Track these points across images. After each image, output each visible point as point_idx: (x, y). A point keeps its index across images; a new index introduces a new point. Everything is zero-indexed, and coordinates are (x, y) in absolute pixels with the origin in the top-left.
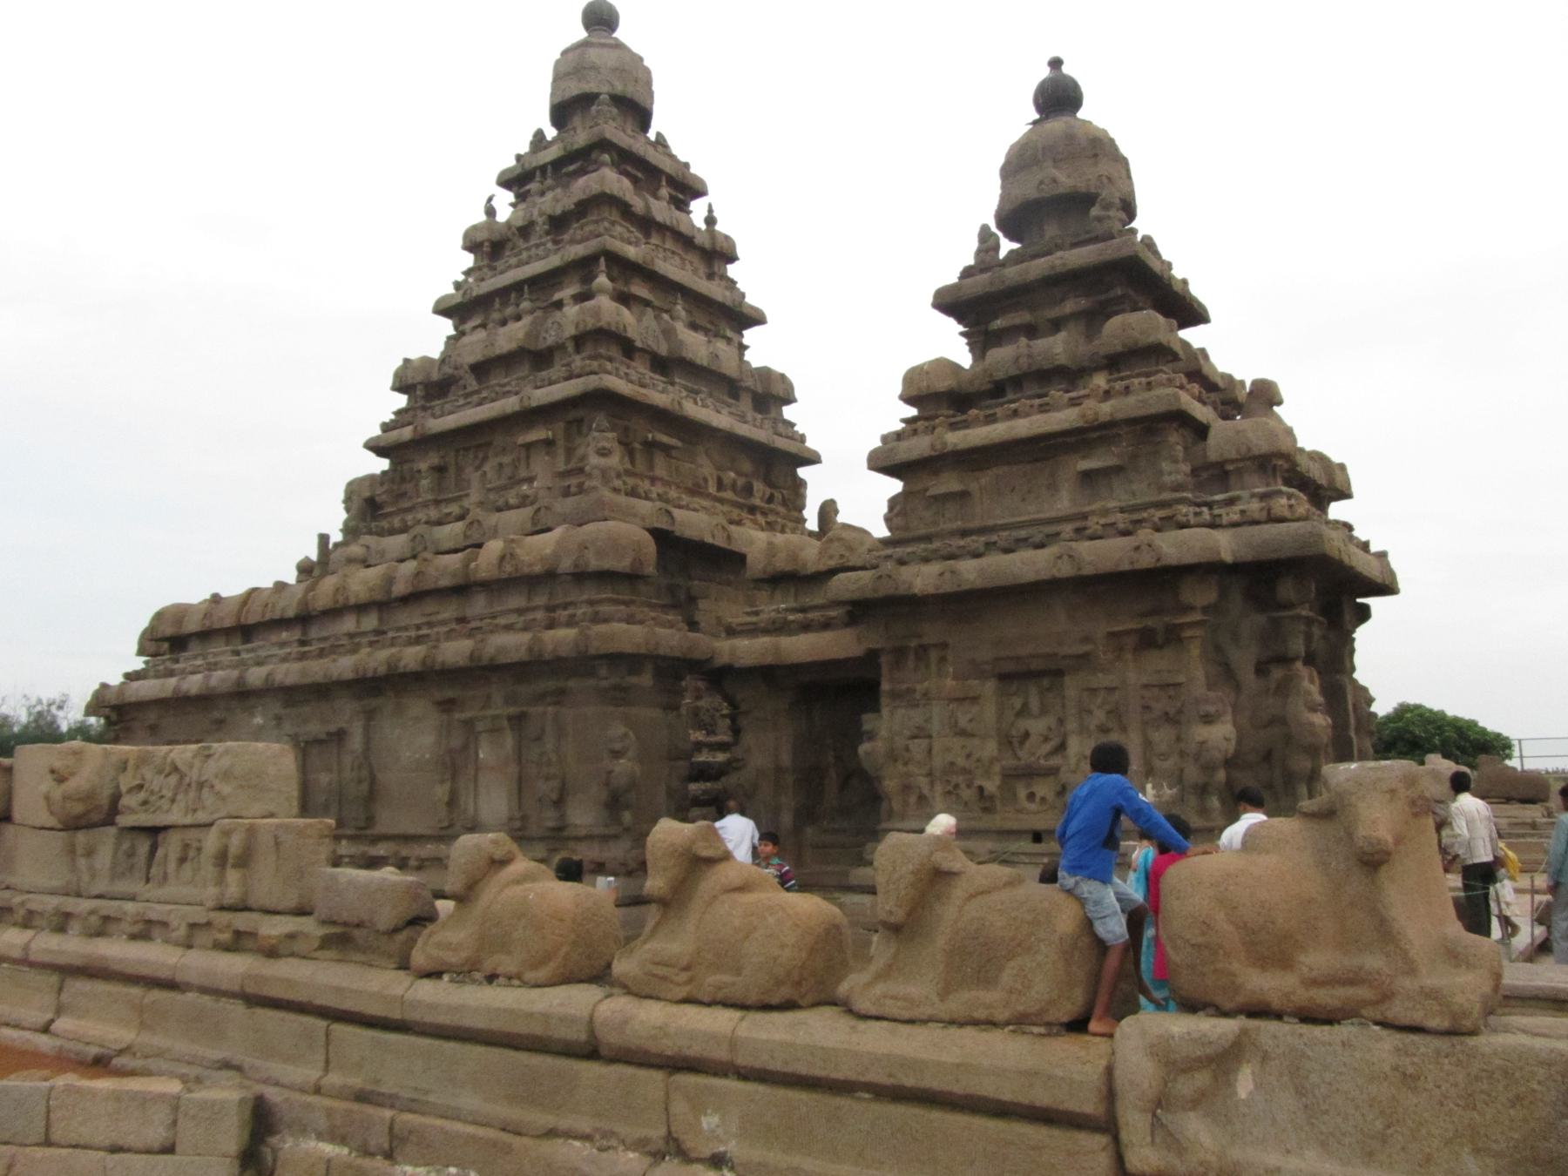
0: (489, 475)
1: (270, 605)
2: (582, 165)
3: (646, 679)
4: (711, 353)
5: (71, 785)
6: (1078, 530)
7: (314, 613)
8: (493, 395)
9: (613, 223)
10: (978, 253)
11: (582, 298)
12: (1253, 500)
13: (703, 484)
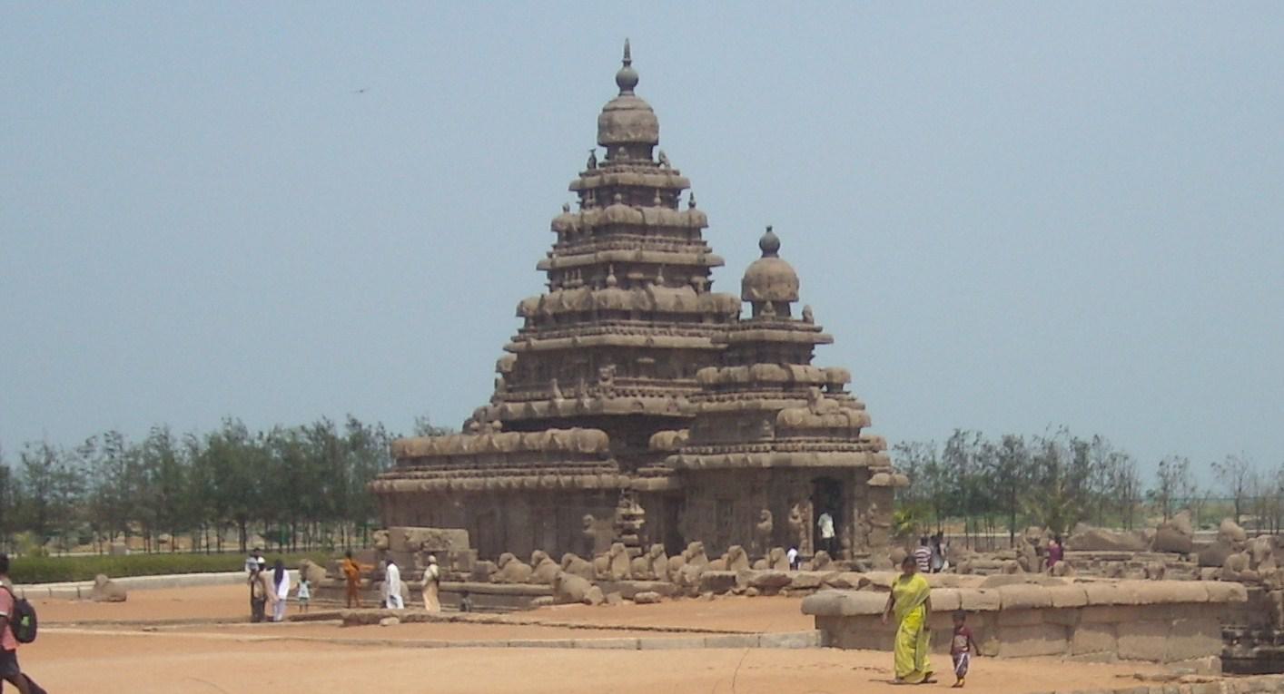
3: (602, 496)
5: (412, 540)
11: (605, 285)
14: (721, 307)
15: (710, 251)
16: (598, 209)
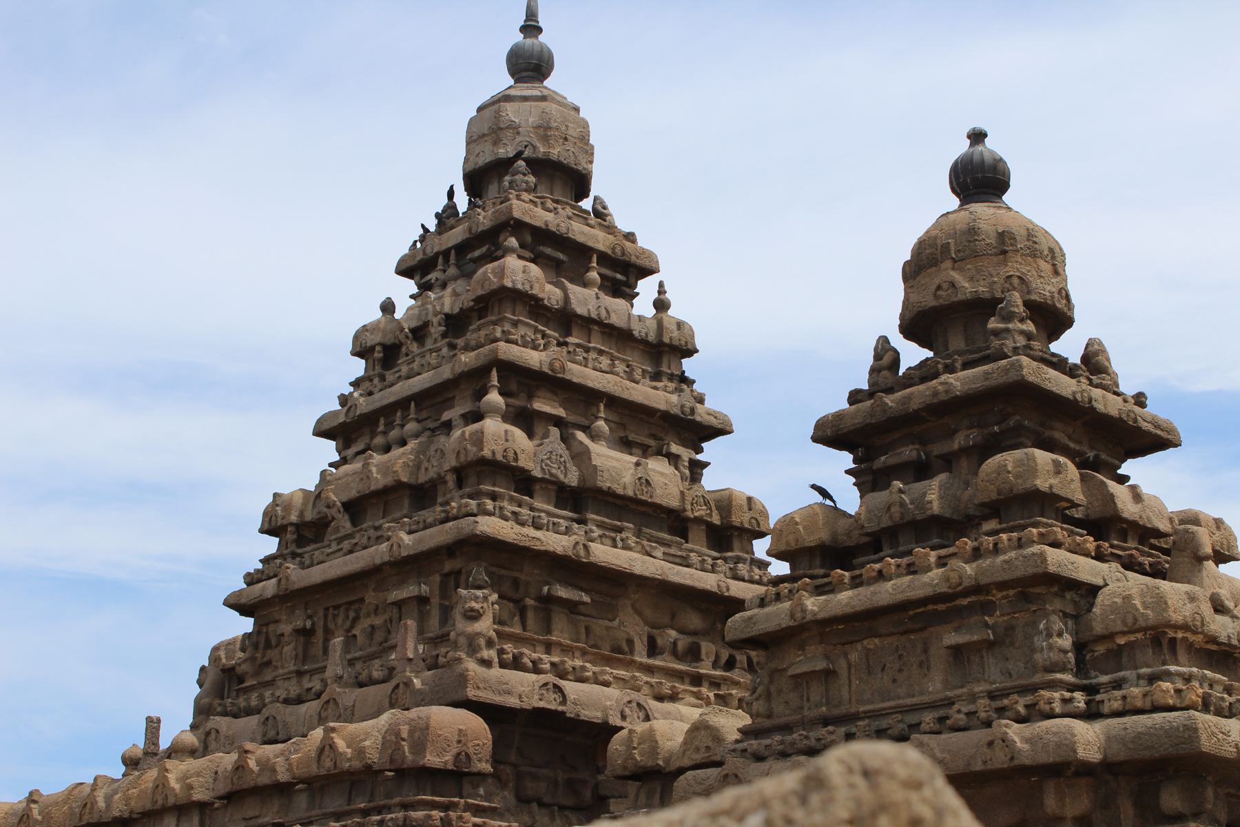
0: (360, 639)
1: (88, 806)
2: (488, 250)
4: (640, 479)
6: (942, 720)
7: (135, 816)
8: (364, 541)
9: (515, 324)
10: (874, 371)
12: (1141, 682)
13: (626, 649)
14: (729, 512)
15: (700, 400)
16: (460, 285)
